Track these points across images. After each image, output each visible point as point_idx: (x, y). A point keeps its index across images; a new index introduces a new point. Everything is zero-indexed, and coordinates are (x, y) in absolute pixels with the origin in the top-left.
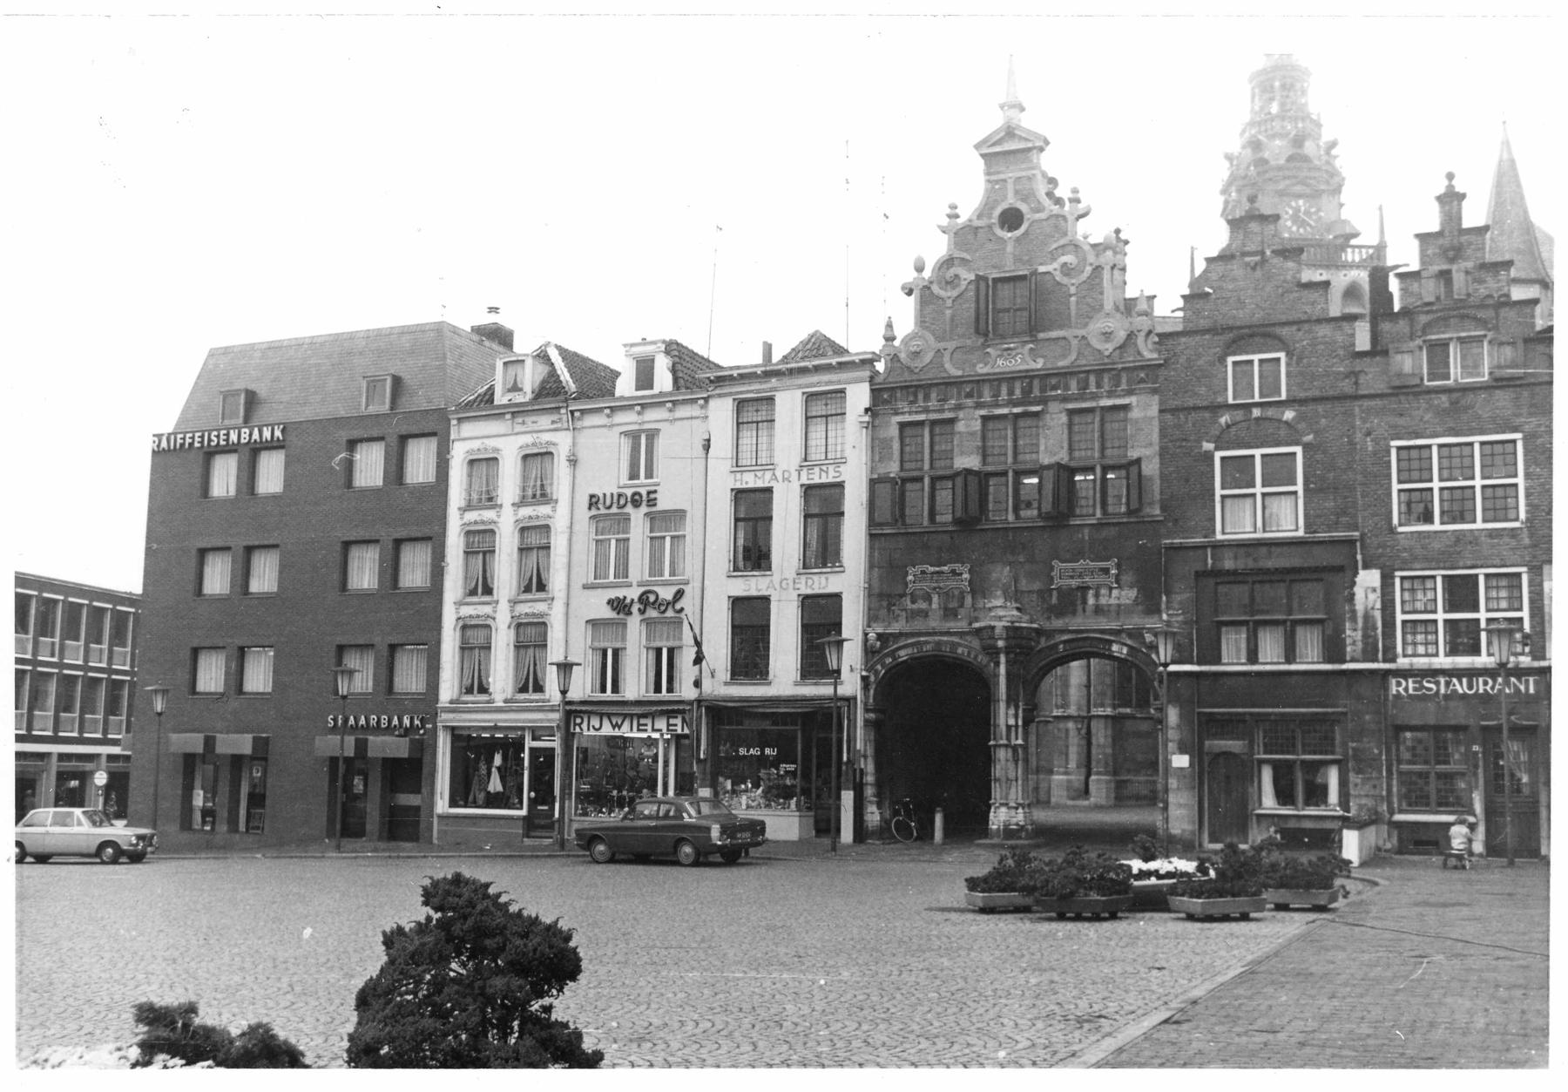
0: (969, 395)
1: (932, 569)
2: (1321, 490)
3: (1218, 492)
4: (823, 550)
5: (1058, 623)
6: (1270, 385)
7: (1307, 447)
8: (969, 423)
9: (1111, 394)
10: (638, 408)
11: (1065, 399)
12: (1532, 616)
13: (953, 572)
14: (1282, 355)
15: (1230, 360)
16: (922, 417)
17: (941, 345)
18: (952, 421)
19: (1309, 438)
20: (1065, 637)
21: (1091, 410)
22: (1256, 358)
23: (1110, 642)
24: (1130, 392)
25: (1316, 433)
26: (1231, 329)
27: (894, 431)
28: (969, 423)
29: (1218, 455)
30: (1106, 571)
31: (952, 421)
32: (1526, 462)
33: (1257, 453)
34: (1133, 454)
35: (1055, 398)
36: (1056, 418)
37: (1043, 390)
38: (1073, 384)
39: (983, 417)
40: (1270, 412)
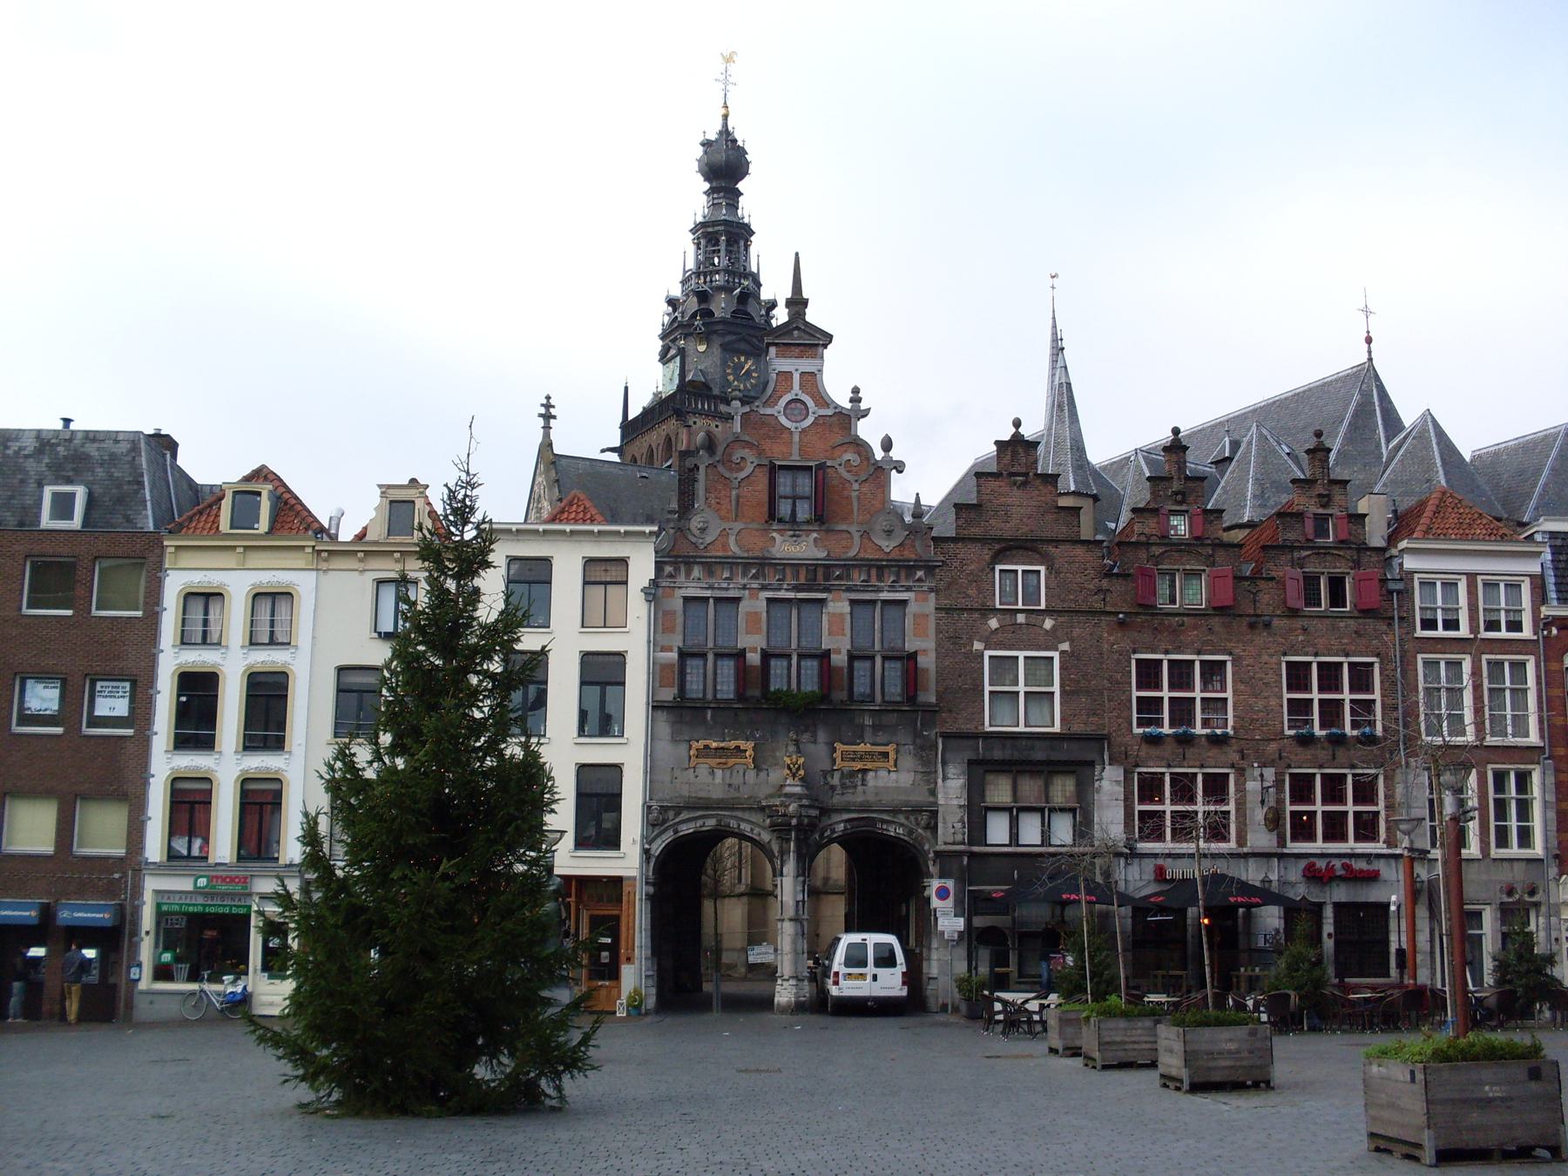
0: (755, 577)
1: (714, 745)
2: (1072, 693)
3: (987, 688)
4: (599, 719)
5: (837, 800)
6: (1031, 595)
7: (1062, 652)
8: (754, 604)
9: (892, 589)
10: (397, 555)
11: (849, 589)
12: (1237, 810)
14: (1042, 569)
15: (998, 567)
16: (708, 593)
17: (726, 525)
18: (737, 600)
19: (1065, 646)
20: (846, 816)
21: (874, 602)
22: (1020, 568)
23: (883, 821)
24: (909, 589)
25: (1072, 641)
26: (999, 540)
27: (678, 604)
28: (754, 604)
29: (988, 653)
30: (886, 755)
31: (737, 600)
32: (1234, 681)
33: (1021, 655)
34: (910, 646)
35: (839, 589)
36: (839, 606)
37: (827, 578)
38: (855, 574)
39: (769, 600)
40: (1033, 619)
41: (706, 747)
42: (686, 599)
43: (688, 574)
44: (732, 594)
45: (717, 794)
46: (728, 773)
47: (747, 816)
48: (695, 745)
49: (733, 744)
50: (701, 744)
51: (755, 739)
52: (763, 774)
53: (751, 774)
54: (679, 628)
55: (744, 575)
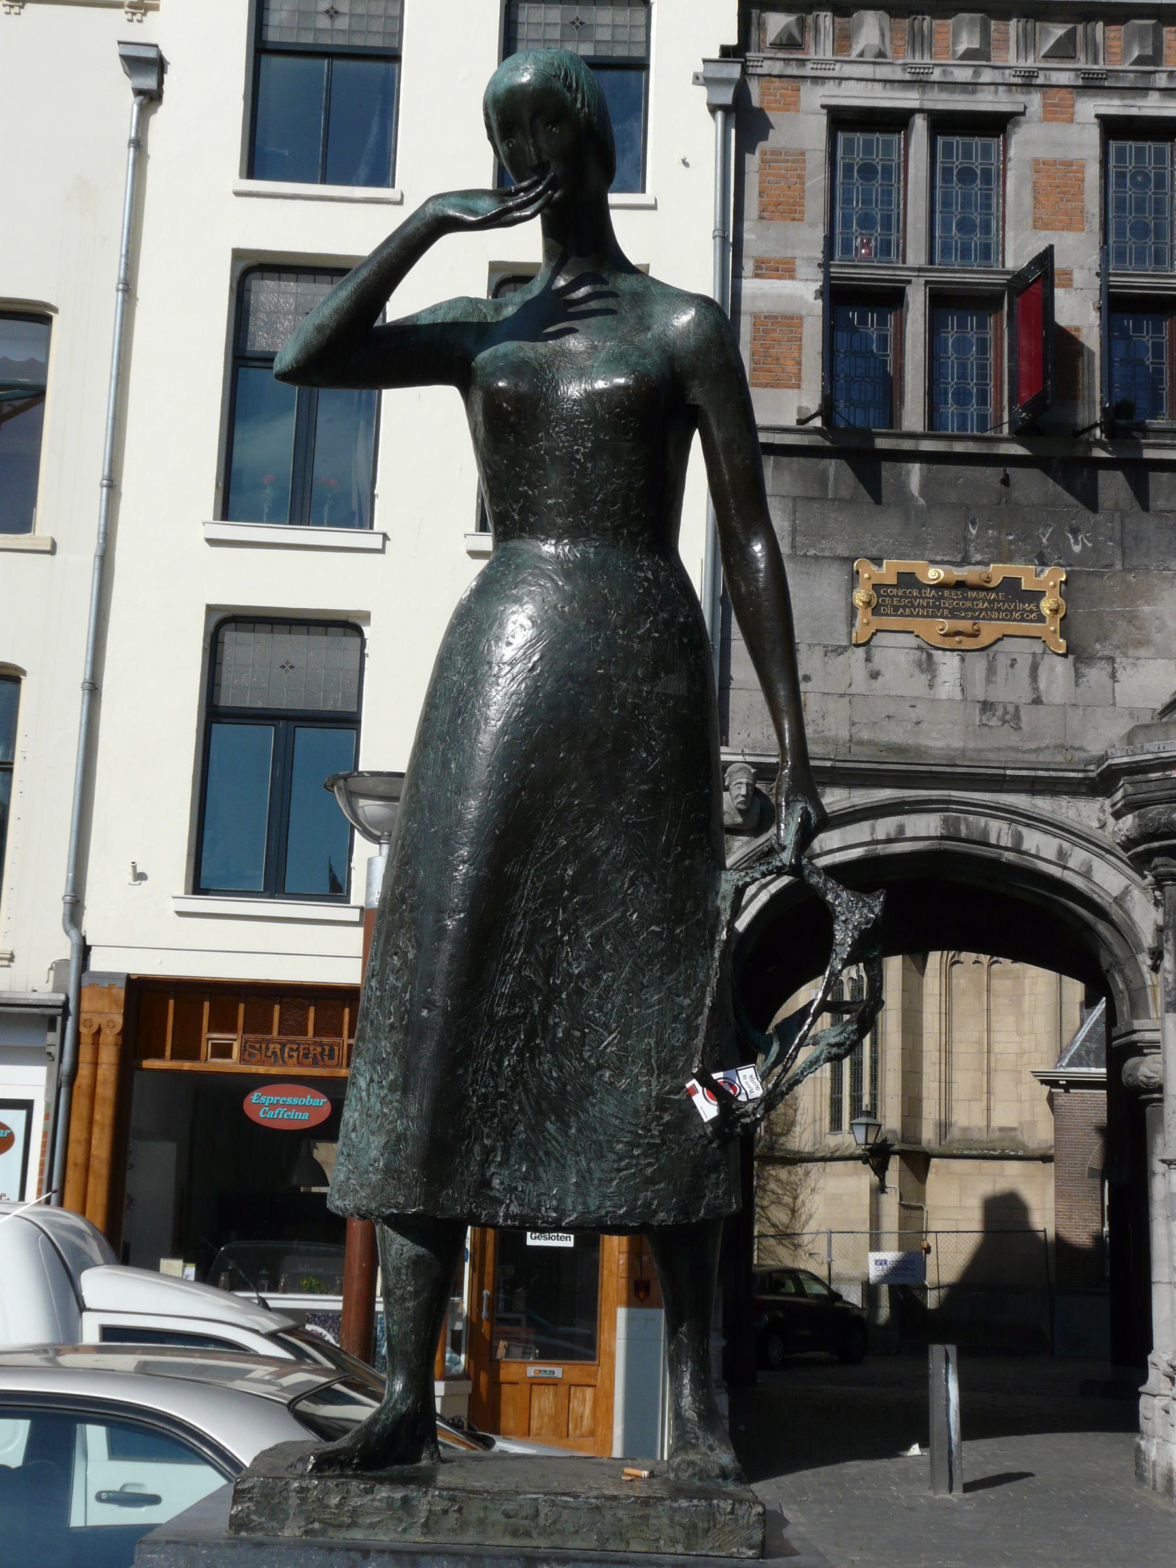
1: (934, 574)
13: (1011, 585)
41: (907, 580)
42: (842, 120)
43: (843, 41)
44: (987, 102)
45: (944, 737)
46: (979, 664)
47: (1043, 805)
48: (867, 572)
49: (997, 572)
50: (887, 572)
51: (1066, 558)
52: (1096, 674)
53: (1057, 674)
54: (816, 206)
55: (1027, 43)
